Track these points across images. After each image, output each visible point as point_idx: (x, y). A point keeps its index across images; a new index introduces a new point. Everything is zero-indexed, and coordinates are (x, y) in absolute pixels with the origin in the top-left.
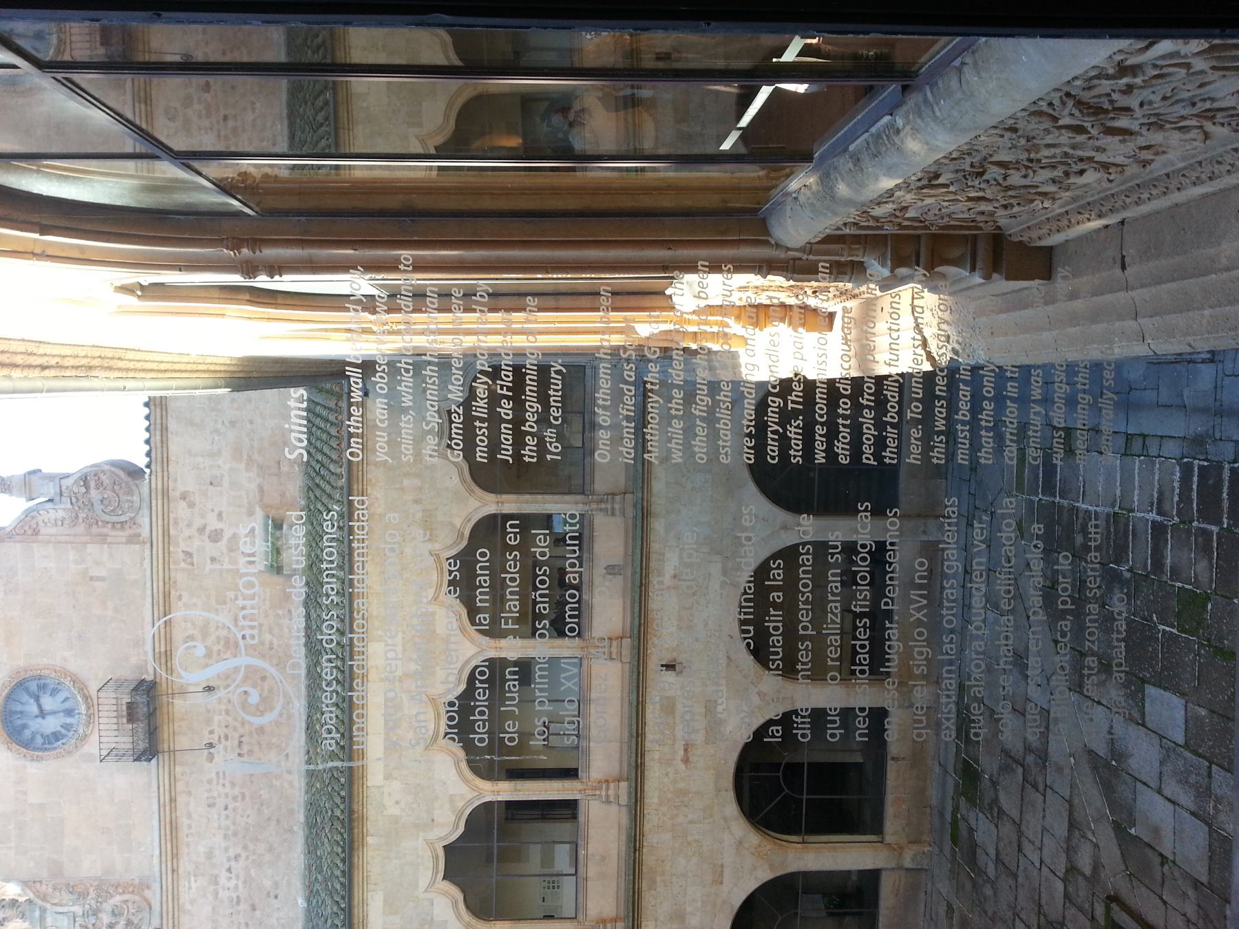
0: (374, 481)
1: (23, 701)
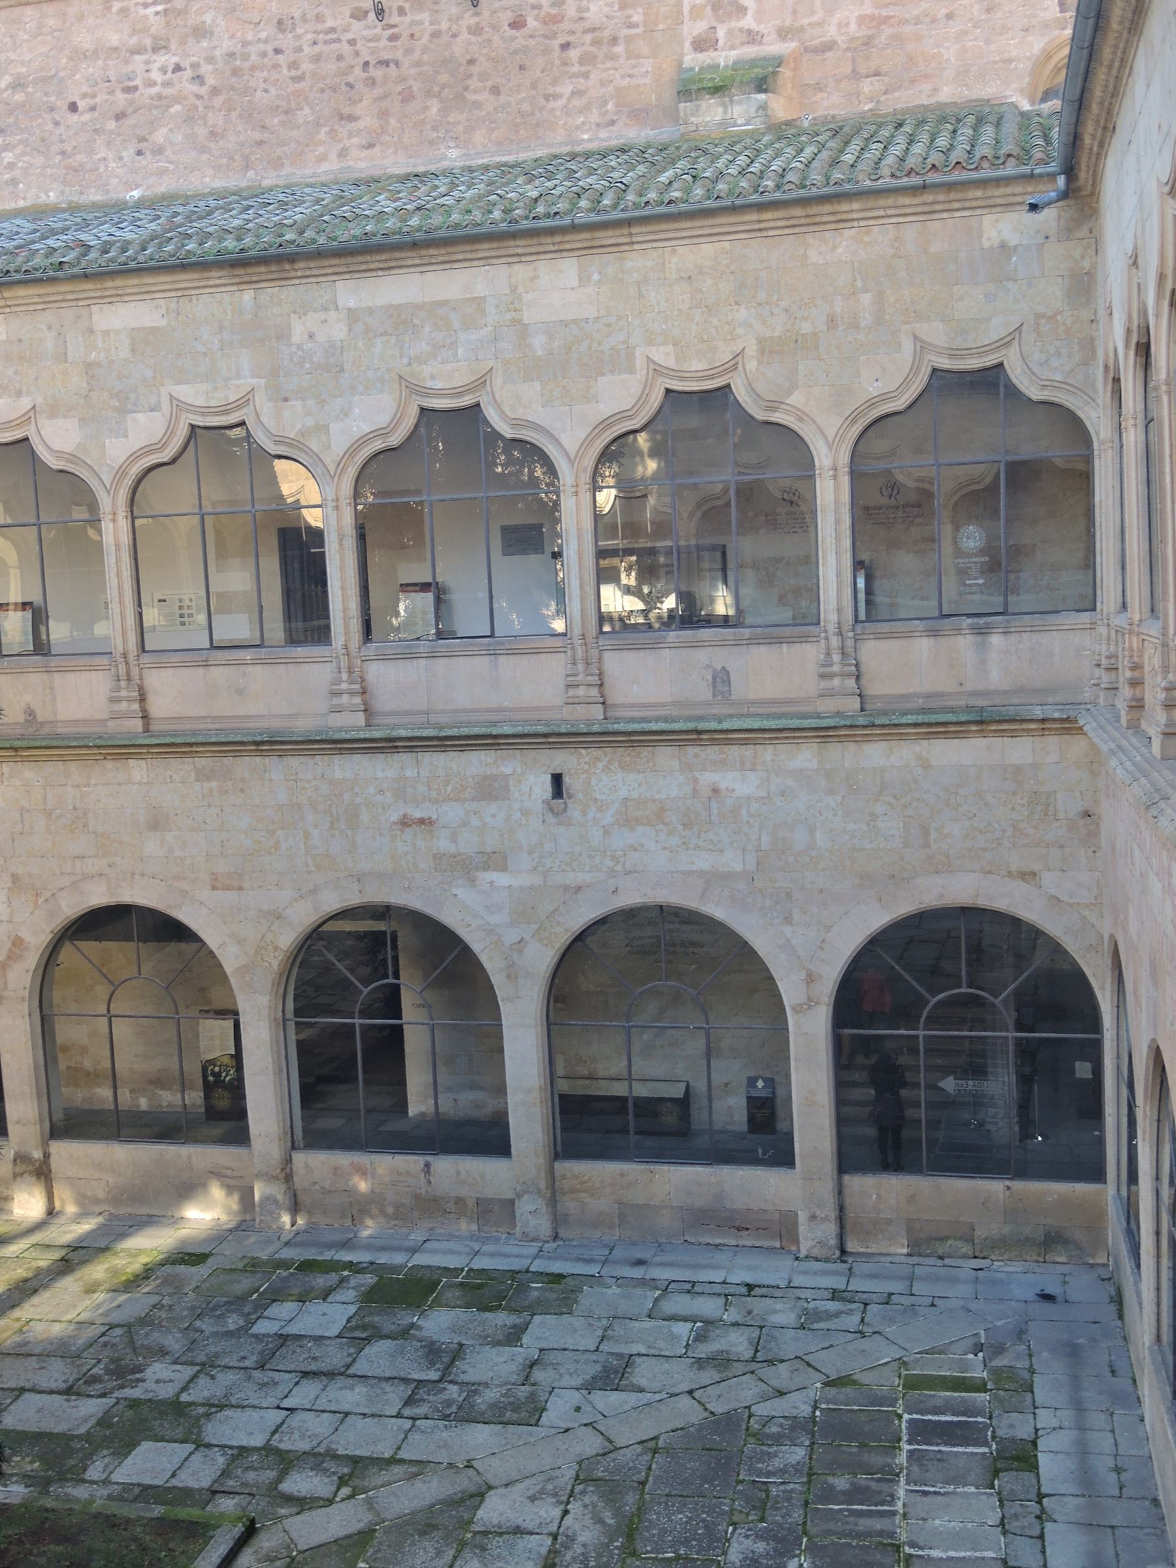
0: (866, 239)
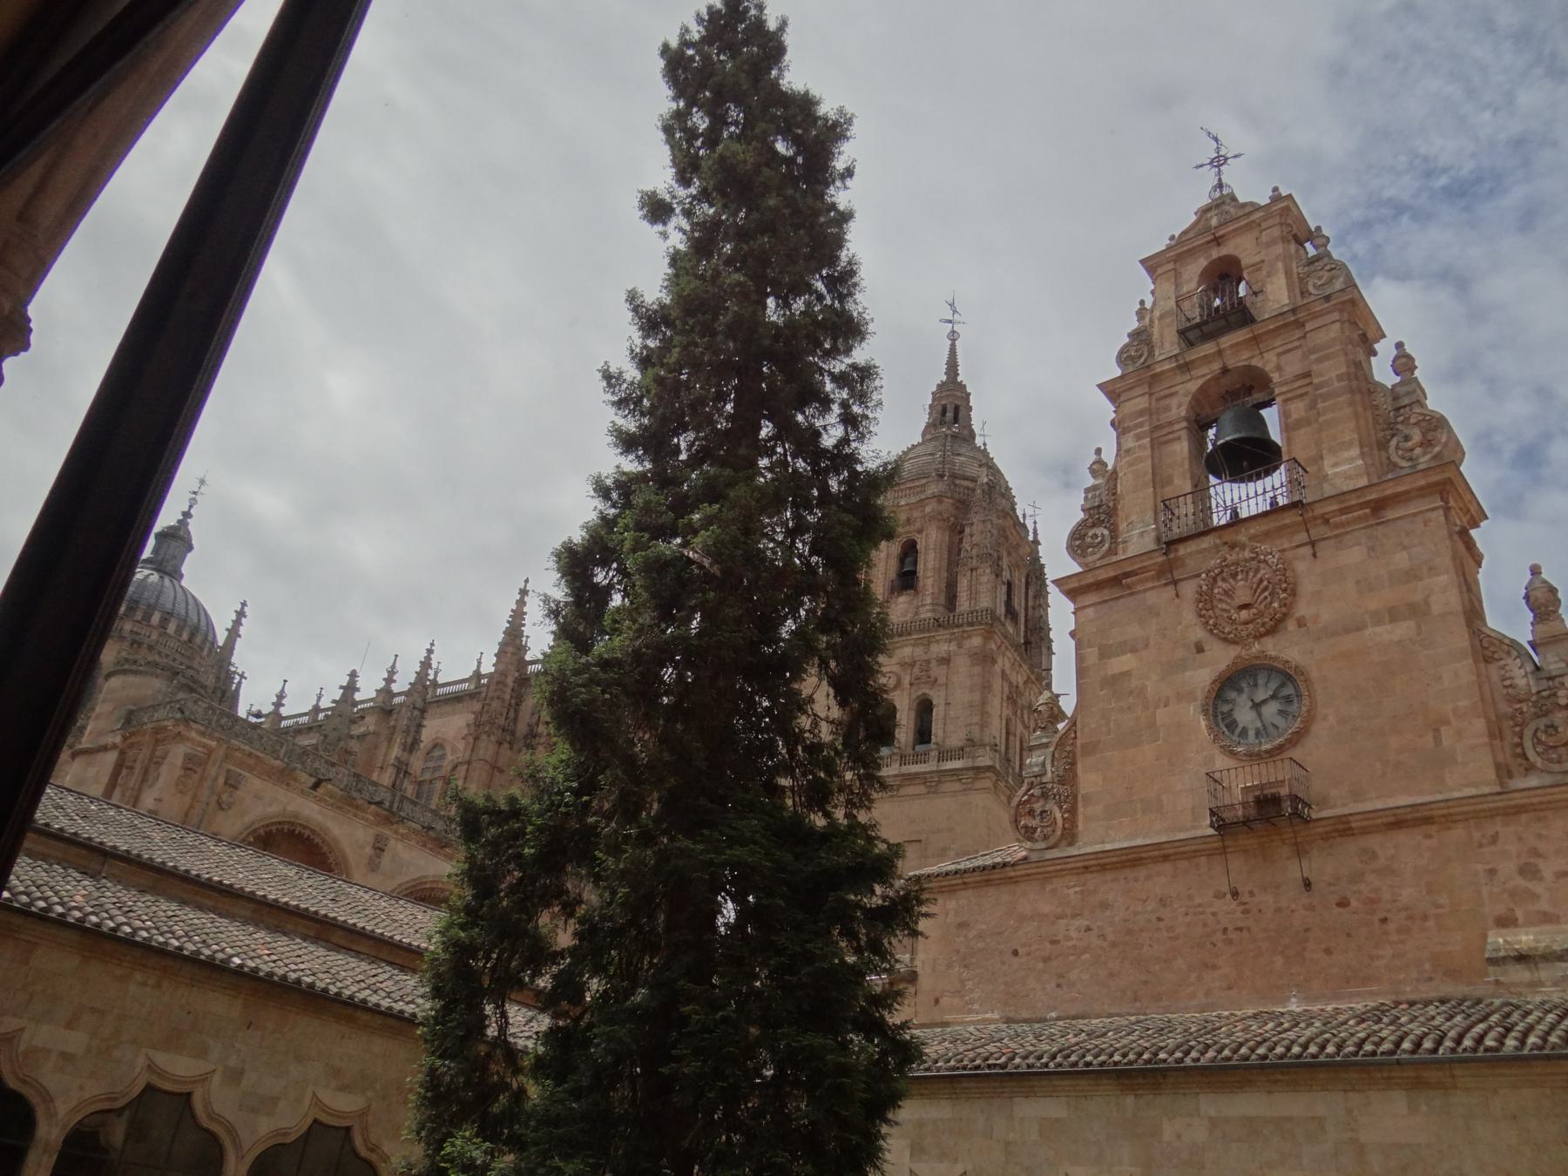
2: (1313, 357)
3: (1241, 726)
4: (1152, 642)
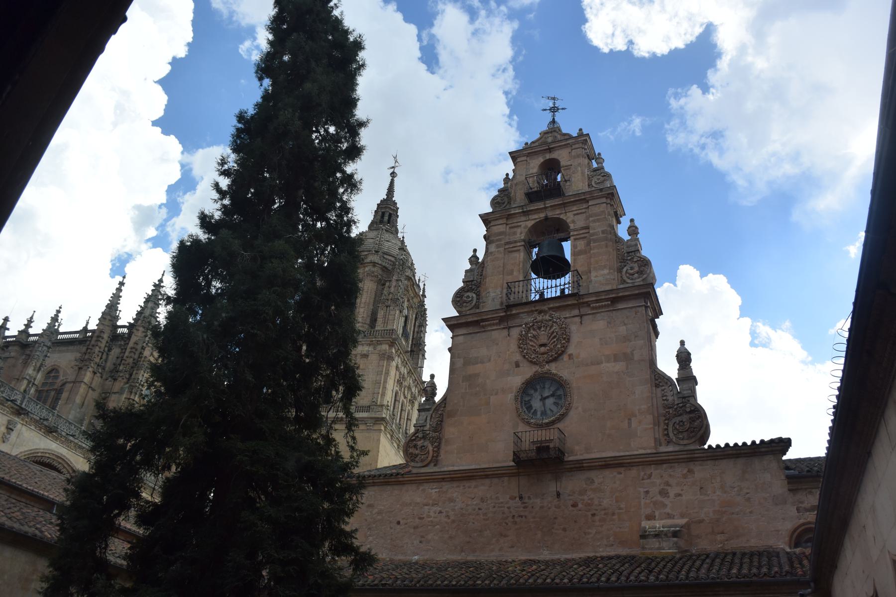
1: (551, 388)
2: (591, 219)
3: (534, 409)
4: (492, 359)
